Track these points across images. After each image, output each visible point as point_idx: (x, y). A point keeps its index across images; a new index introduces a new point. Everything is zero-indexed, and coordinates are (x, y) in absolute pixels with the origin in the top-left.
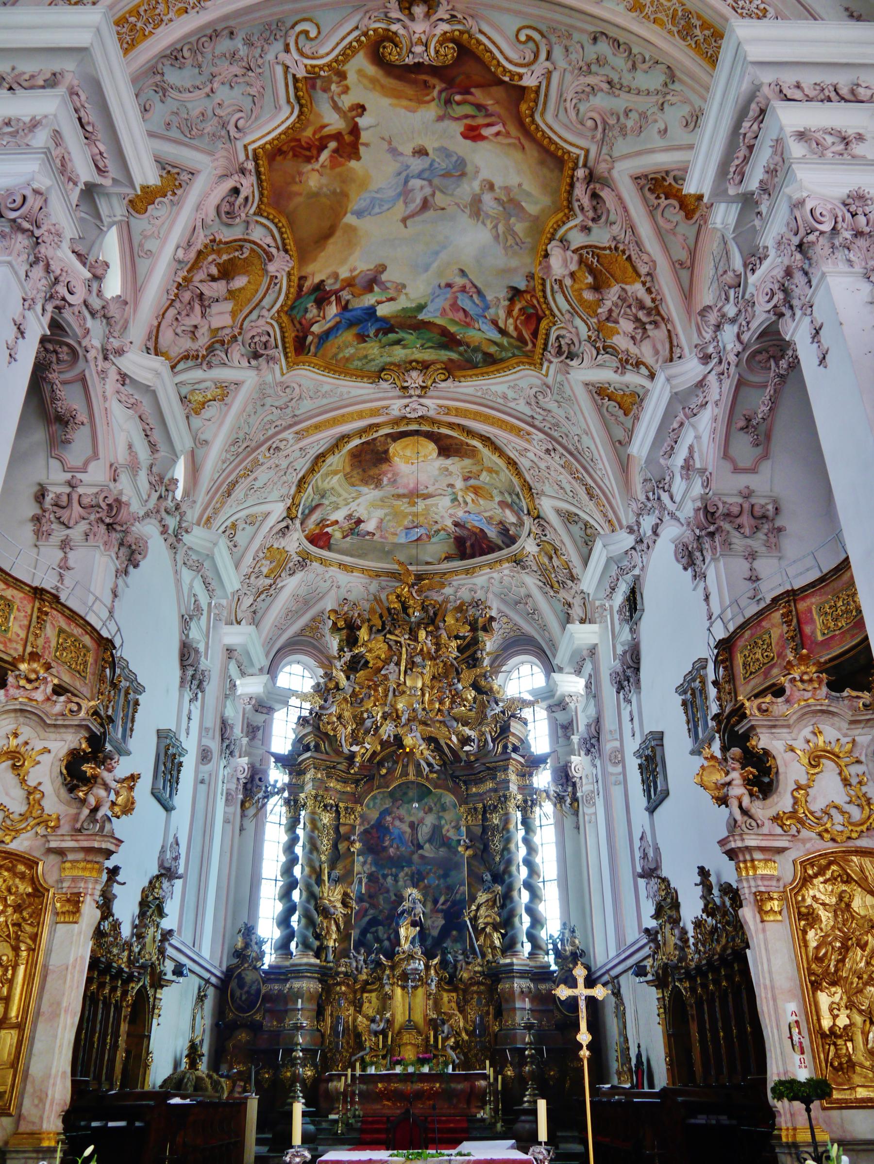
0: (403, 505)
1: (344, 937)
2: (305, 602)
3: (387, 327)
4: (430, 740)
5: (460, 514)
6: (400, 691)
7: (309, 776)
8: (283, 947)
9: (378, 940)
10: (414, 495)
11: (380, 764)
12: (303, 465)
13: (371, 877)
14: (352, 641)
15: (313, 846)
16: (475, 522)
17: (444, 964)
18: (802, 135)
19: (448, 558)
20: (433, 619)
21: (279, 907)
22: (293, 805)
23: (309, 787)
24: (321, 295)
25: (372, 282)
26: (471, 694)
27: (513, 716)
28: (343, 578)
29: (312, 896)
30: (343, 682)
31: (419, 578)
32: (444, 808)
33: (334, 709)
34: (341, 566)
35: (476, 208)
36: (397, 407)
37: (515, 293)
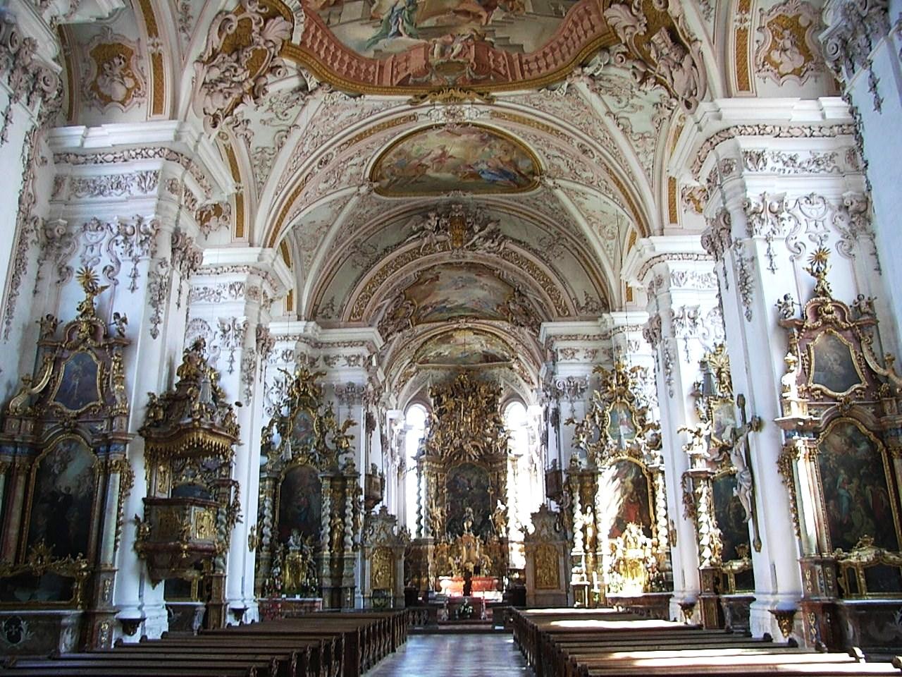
0: (460, 347)
1: (442, 527)
2: (416, 384)
3: (451, 309)
4: (475, 447)
5: (485, 349)
6: (461, 424)
7: (425, 464)
8: (419, 532)
9: (456, 527)
10: (464, 344)
11: (454, 456)
12: (417, 347)
13: (452, 502)
14: (439, 402)
15: (428, 494)
16: (491, 351)
17: (482, 538)
18: (562, 351)
19: (481, 362)
20: (474, 390)
21: (417, 517)
22: (419, 475)
23: (425, 469)
24: (425, 308)
25: (443, 302)
26: (492, 424)
27: (509, 437)
28: (434, 372)
29: (429, 513)
30: (437, 420)
31: (468, 370)
32: (481, 472)
33: (434, 437)
34: (433, 368)
35: (482, 288)
36: (455, 326)
37: (498, 306)
